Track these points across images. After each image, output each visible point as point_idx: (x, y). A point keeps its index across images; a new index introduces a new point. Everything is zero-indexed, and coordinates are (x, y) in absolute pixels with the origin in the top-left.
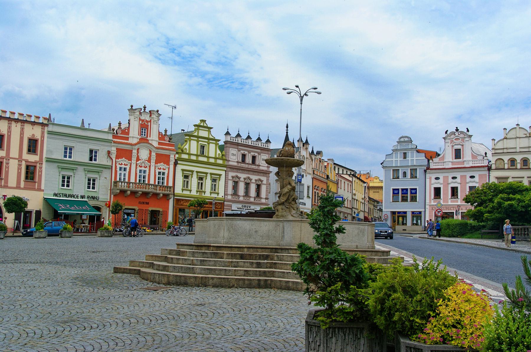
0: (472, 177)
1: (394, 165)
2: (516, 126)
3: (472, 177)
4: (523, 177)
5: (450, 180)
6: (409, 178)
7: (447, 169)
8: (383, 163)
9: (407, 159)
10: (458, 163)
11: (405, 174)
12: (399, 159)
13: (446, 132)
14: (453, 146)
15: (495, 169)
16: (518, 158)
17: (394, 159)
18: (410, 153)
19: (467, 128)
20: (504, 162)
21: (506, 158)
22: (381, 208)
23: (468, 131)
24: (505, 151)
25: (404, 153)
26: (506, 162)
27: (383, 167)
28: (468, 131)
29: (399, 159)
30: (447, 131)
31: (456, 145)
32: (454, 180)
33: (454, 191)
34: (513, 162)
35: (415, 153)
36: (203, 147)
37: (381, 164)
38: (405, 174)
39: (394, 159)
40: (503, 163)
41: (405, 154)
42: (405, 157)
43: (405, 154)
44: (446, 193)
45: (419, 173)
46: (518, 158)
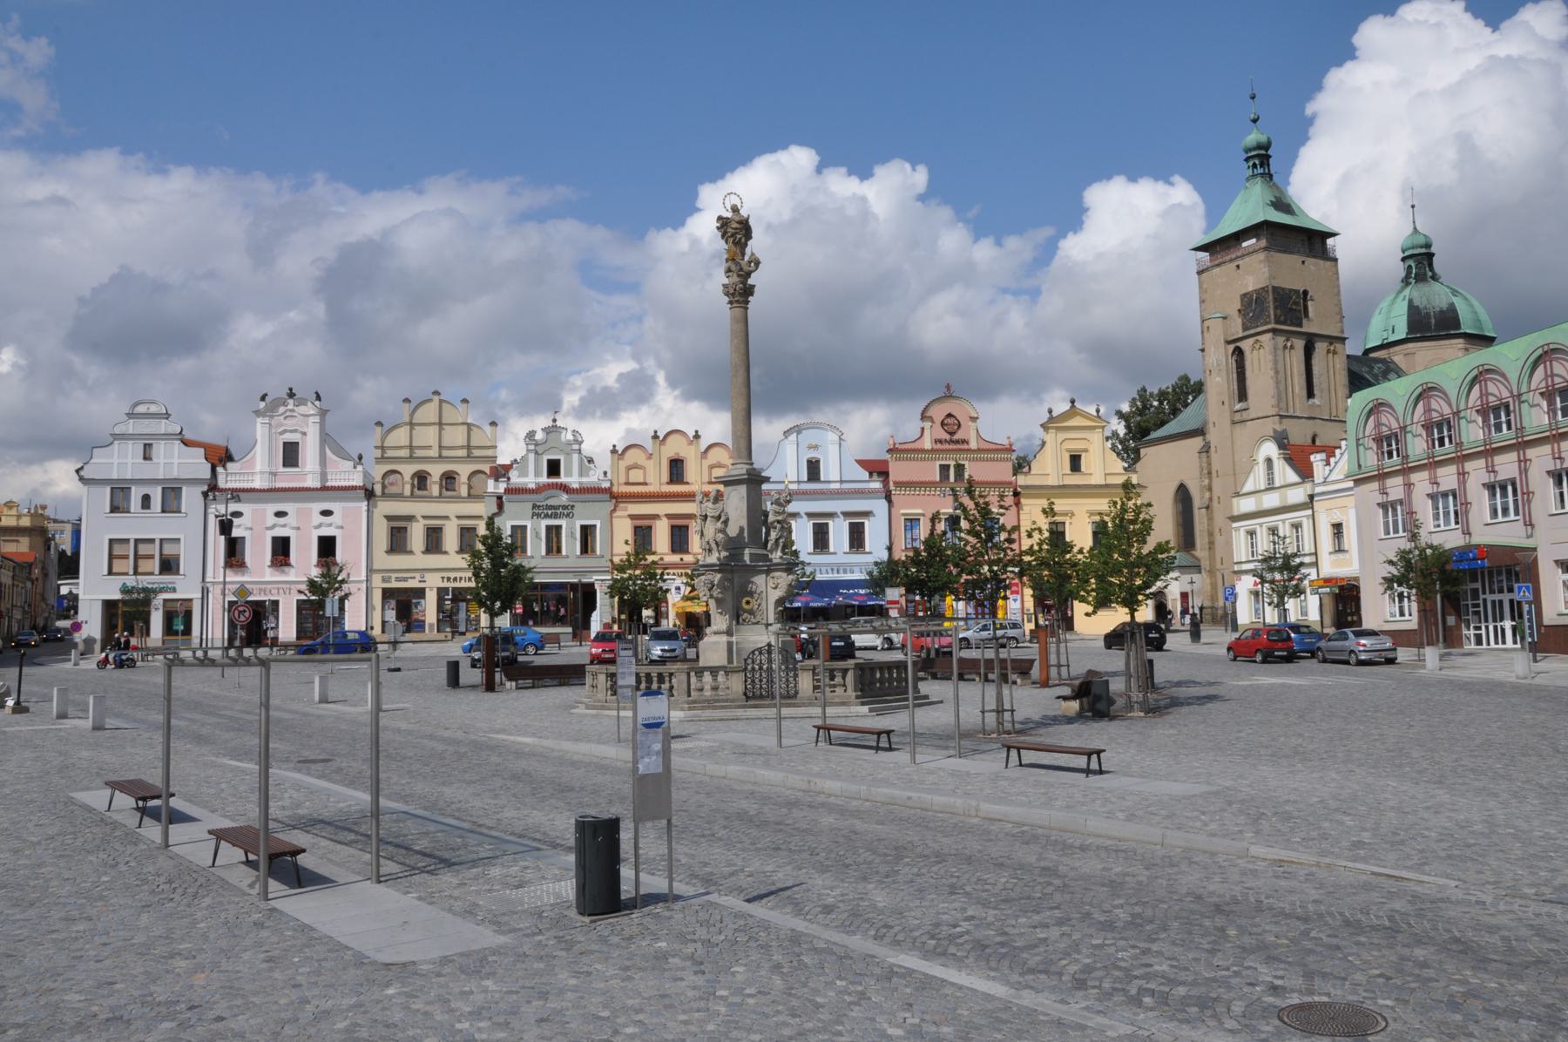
0: (327, 513)
1: (115, 476)
2: (431, 396)
3: (327, 513)
4: (446, 518)
5: (272, 520)
6: (159, 509)
8: (82, 468)
9: (155, 460)
12: (130, 460)
13: (263, 398)
16: (436, 471)
17: (115, 461)
18: (162, 446)
19: (317, 393)
21: (408, 470)
22: (75, 591)
25: (145, 445)
26: (407, 478)
27: (81, 479)
29: (130, 460)
30: (266, 395)
32: (282, 520)
33: (281, 549)
34: (421, 479)
35: (176, 446)
37: (77, 471)
39: (115, 461)
40: (400, 483)
41: (148, 447)
42: (147, 457)
43: (148, 447)
45: (191, 498)
46: (436, 471)
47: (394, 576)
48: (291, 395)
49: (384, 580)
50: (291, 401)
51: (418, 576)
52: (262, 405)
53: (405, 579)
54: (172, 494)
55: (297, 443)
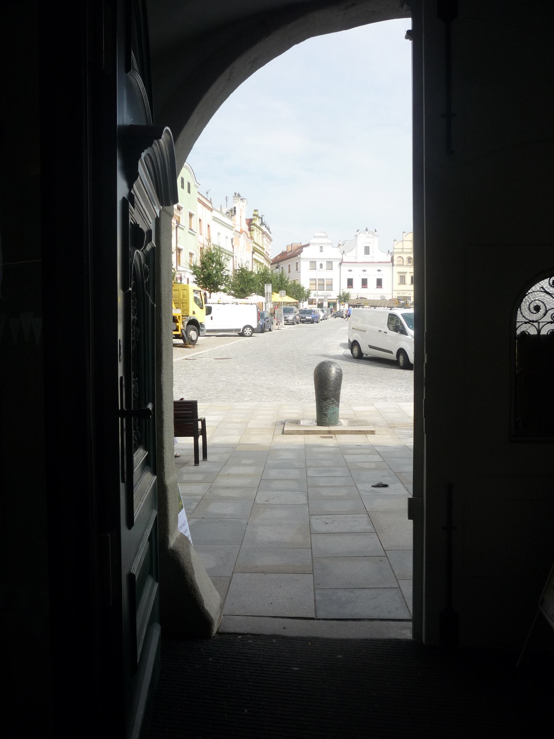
7: (359, 263)
10: (367, 258)
11: (321, 265)
13: (358, 231)
14: (363, 244)
15: (397, 265)
19: (375, 230)
20: (403, 259)
23: (376, 231)
24: (405, 251)
28: (376, 231)
30: (359, 230)
31: (366, 242)
36: (258, 235)
38: (321, 265)
40: (402, 261)
41: (321, 247)
43: (321, 247)
44: (357, 283)
45: (336, 264)
47: (401, 292)
48: (367, 230)
49: (398, 294)
50: (367, 232)
51: (408, 292)
52: (358, 233)
53: (404, 293)
54: (330, 264)
55: (369, 247)
